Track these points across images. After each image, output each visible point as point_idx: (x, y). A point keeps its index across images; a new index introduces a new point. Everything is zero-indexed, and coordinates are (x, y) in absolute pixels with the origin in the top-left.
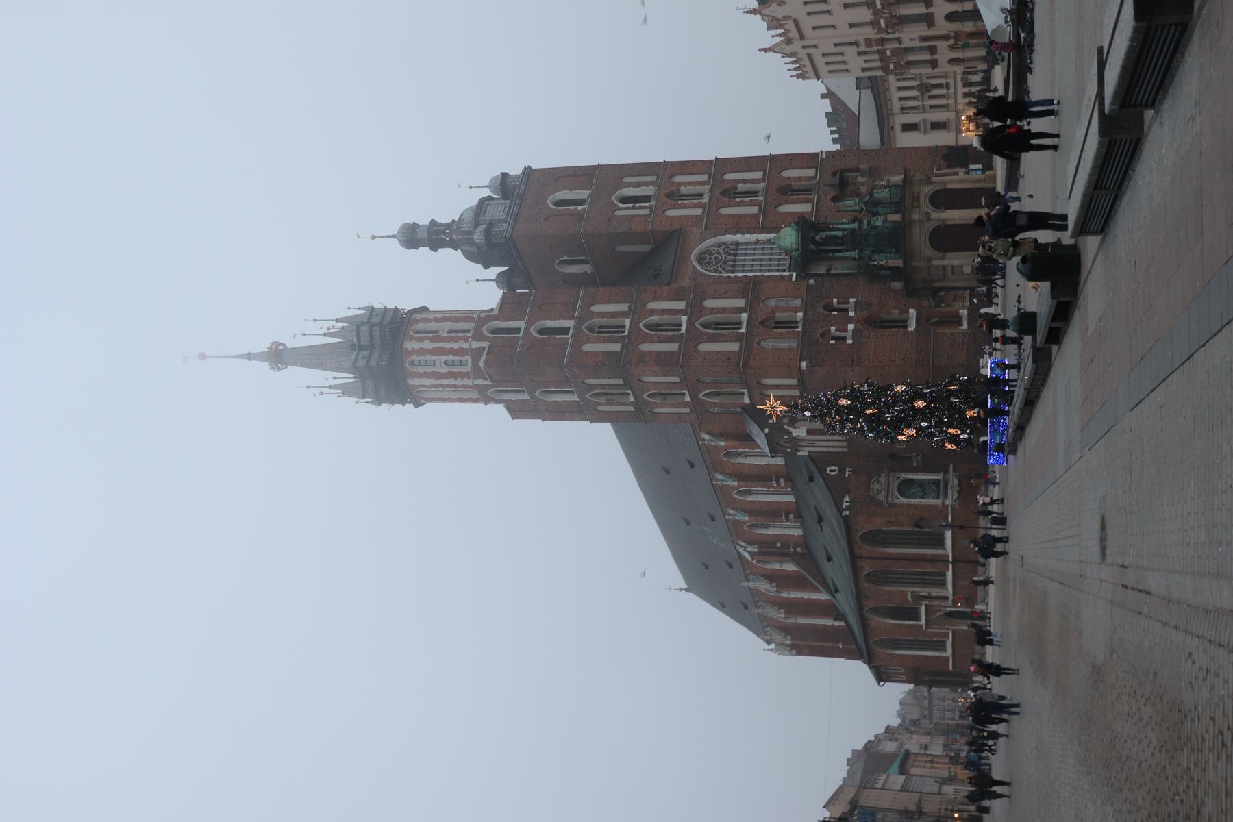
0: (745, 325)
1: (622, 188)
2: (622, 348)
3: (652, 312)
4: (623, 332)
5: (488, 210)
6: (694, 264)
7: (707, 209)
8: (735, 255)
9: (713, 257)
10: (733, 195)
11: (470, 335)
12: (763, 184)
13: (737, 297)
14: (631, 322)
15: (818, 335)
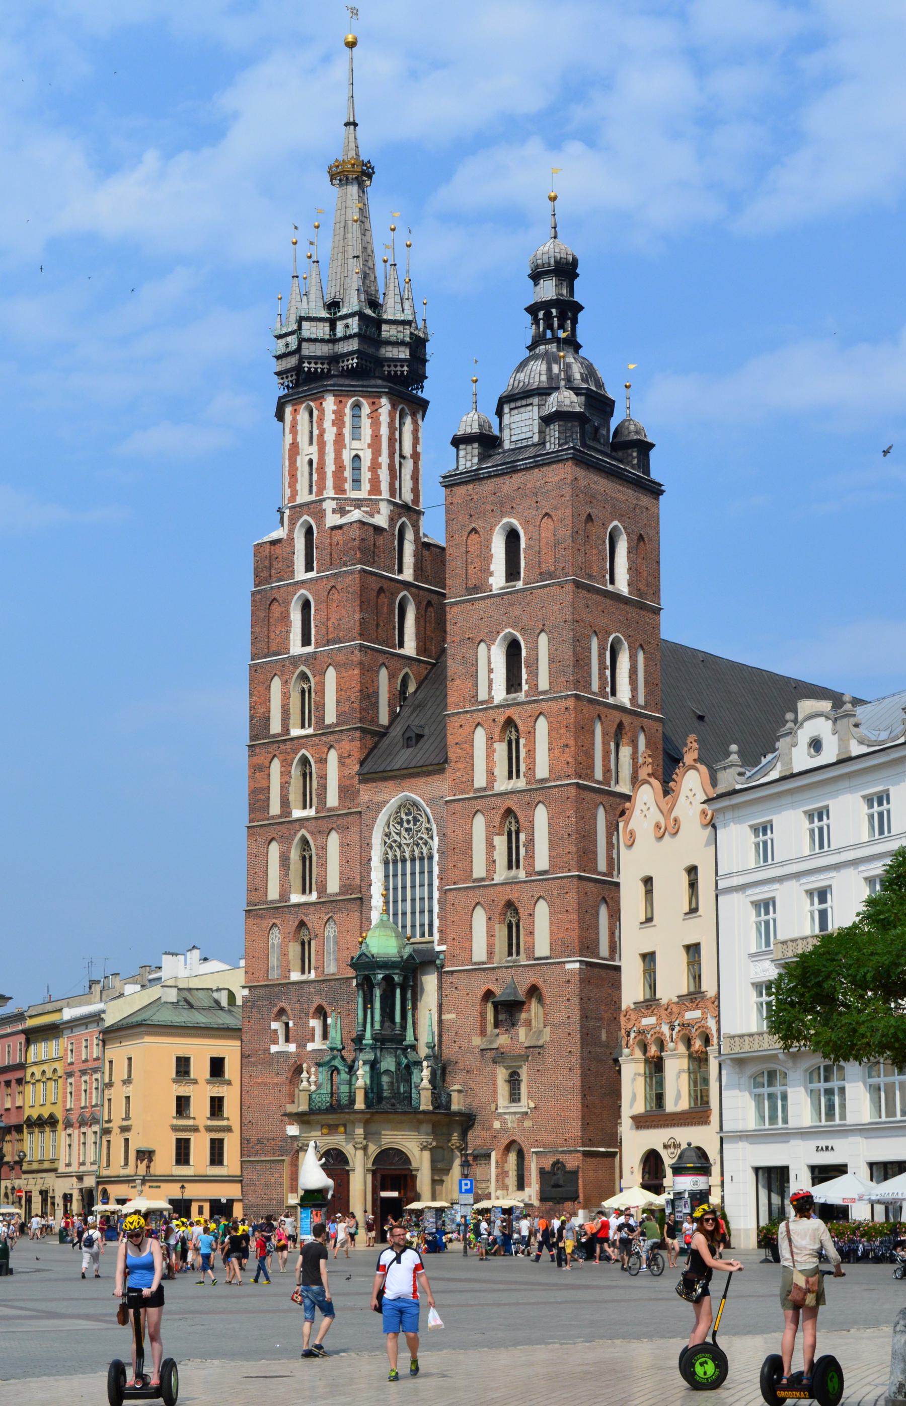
0: (303, 899)
1: (524, 640)
2: (274, 736)
3: (323, 761)
4: (303, 726)
5: (522, 410)
6: (392, 801)
7: (482, 795)
8: (413, 860)
9: (411, 825)
10: (513, 829)
11: (303, 497)
12: (522, 874)
13: (340, 879)
14: (307, 736)
15: (282, 1004)
